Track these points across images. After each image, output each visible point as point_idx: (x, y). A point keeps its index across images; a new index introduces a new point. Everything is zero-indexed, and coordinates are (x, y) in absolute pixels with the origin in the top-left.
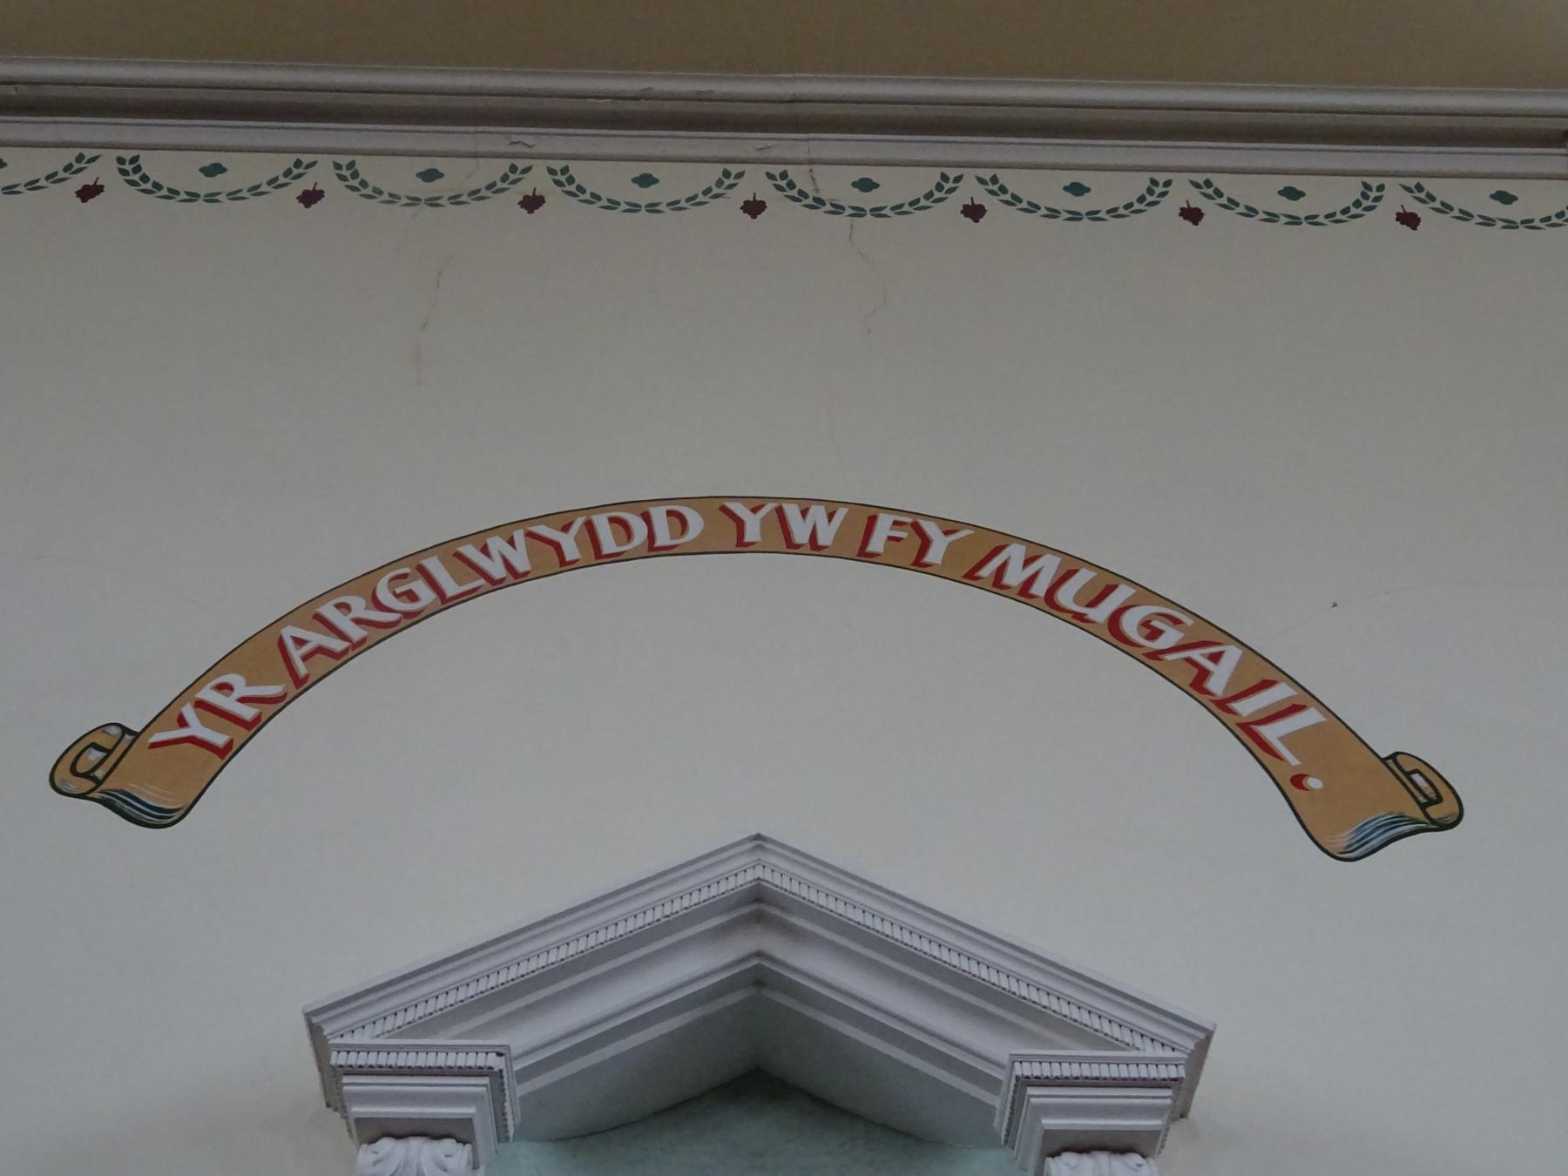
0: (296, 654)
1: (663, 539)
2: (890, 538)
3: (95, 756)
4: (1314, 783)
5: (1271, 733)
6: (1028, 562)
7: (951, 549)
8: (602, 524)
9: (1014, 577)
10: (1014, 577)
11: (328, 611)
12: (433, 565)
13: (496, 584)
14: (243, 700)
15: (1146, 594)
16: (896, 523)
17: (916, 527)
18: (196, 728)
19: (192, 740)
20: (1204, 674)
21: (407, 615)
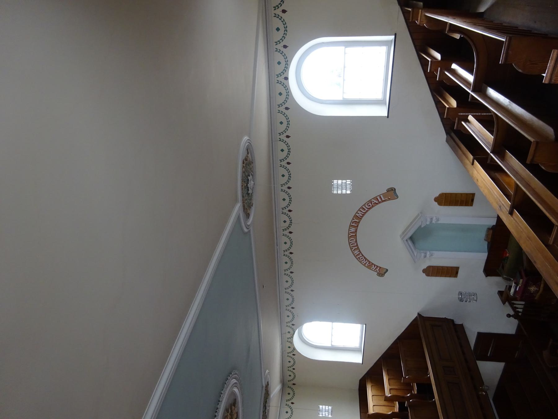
0: (369, 265)
2: (355, 224)
4: (389, 198)
5: (383, 199)
7: (356, 219)
9: (361, 215)
10: (361, 215)
11: (364, 263)
12: (357, 257)
13: (361, 252)
14: (374, 267)
15: (364, 205)
16: (353, 223)
17: (353, 222)
18: (378, 270)
19: (379, 270)
20: (375, 203)
21: (364, 258)
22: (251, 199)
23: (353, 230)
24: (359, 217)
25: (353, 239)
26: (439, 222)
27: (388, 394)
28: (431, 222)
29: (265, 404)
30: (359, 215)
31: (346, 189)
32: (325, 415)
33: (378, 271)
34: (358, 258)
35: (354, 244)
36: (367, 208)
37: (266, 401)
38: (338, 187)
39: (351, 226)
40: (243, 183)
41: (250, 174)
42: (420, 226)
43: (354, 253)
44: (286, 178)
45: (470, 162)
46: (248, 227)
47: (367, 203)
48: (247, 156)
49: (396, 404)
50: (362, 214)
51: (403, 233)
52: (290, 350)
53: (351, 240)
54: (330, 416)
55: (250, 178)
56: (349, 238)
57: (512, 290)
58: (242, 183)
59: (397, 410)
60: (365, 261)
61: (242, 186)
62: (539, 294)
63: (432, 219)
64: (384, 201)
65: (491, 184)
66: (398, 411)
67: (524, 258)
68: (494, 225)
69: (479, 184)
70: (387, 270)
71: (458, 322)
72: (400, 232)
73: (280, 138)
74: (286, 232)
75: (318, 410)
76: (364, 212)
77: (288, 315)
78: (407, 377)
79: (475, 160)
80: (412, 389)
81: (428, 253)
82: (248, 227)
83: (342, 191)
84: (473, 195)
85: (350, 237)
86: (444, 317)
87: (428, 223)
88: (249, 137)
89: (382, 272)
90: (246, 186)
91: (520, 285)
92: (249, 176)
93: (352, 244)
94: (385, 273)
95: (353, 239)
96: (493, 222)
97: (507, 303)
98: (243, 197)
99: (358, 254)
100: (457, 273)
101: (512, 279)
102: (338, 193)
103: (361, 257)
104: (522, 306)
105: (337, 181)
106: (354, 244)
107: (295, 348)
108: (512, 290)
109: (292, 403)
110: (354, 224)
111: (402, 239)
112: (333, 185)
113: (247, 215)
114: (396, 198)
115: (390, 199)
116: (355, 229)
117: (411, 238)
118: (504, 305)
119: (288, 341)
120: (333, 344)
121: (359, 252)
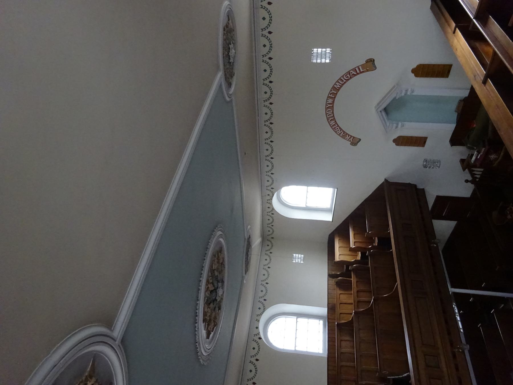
0: (344, 135)
1: (332, 112)
2: (332, 95)
3: (353, 144)
4: (368, 69)
5: (361, 71)
6: (337, 85)
7: (334, 91)
8: (328, 116)
9: (339, 87)
10: (339, 87)
11: (339, 133)
13: (336, 123)
14: (348, 137)
15: (343, 76)
16: (330, 95)
17: (331, 93)
18: (351, 139)
19: (352, 139)
20: (353, 74)
21: (340, 128)
22: (233, 69)
23: (330, 101)
24: (337, 89)
25: (331, 110)
26: (414, 94)
27: (352, 246)
28: (406, 94)
29: (247, 253)
30: (337, 86)
31: (325, 58)
32: (298, 261)
33: (352, 141)
34: (334, 128)
35: (331, 115)
36: (345, 79)
37: (248, 251)
38: (317, 56)
39: (329, 97)
40: (224, 51)
41: (231, 42)
42: (395, 98)
43: (331, 123)
44: (267, 48)
45: (452, 30)
46: (230, 96)
47: (345, 75)
48: (228, 23)
49: (359, 254)
50: (340, 86)
51: (378, 104)
52: (270, 210)
53: (328, 111)
54: (302, 262)
55: (231, 46)
56: (326, 109)
57: (474, 158)
58: (223, 52)
59: (359, 258)
60: (340, 131)
61: (223, 54)
62: (497, 162)
63: (407, 91)
64: (362, 72)
65: (470, 53)
66: (360, 259)
67: (490, 129)
68: (466, 97)
69: (457, 54)
70: (360, 140)
71: (420, 187)
72: (375, 102)
73: (261, 5)
74: (267, 103)
75: (292, 257)
76: (342, 83)
77: (268, 180)
78: (370, 232)
79: (457, 28)
80: (374, 241)
81: (400, 124)
82: (230, 96)
83: (321, 60)
84: (450, 66)
85: (327, 108)
86: (408, 182)
87: (403, 94)
88: (230, 2)
89: (355, 142)
90: (228, 54)
91: (481, 154)
92: (231, 44)
93: (328, 115)
94: (358, 142)
95: (331, 110)
96: (465, 93)
97: (467, 170)
98: (224, 65)
99: (334, 125)
100: (425, 142)
101: (475, 148)
102: (317, 62)
103: (336, 127)
104: (480, 173)
105: (317, 49)
106: (331, 115)
107: (274, 208)
108: (474, 158)
109: (271, 253)
110: (331, 96)
111: (377, 110)
112: (313, 54)
113: (229, 84)
114: (375, 69)
115: (368, 71)
116: (332, 100)
117: (385, 110)
118: (464, 171)
119: (267, 203)
120: (308, 205)
121: (335, 123)
